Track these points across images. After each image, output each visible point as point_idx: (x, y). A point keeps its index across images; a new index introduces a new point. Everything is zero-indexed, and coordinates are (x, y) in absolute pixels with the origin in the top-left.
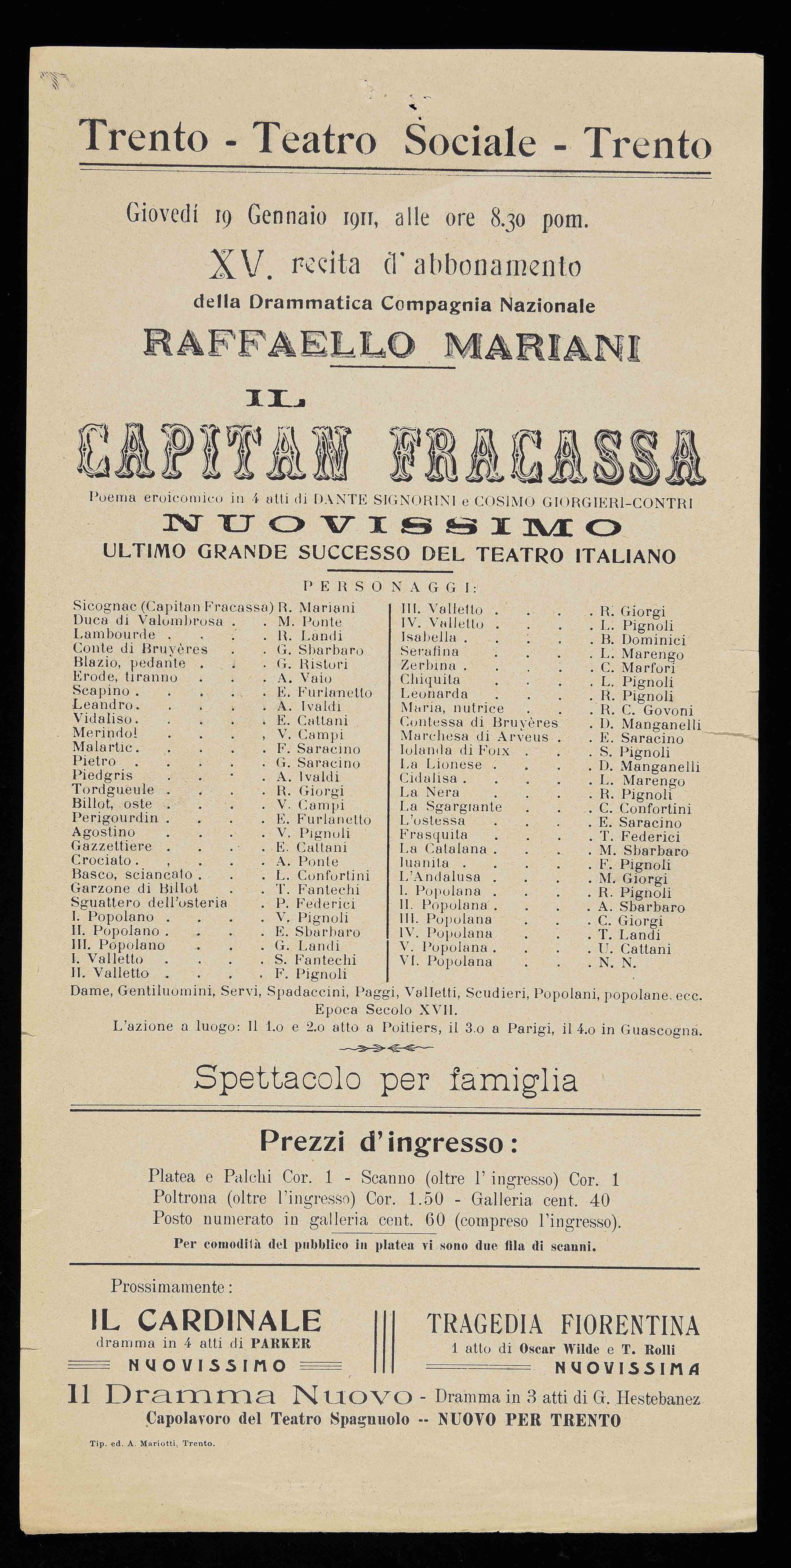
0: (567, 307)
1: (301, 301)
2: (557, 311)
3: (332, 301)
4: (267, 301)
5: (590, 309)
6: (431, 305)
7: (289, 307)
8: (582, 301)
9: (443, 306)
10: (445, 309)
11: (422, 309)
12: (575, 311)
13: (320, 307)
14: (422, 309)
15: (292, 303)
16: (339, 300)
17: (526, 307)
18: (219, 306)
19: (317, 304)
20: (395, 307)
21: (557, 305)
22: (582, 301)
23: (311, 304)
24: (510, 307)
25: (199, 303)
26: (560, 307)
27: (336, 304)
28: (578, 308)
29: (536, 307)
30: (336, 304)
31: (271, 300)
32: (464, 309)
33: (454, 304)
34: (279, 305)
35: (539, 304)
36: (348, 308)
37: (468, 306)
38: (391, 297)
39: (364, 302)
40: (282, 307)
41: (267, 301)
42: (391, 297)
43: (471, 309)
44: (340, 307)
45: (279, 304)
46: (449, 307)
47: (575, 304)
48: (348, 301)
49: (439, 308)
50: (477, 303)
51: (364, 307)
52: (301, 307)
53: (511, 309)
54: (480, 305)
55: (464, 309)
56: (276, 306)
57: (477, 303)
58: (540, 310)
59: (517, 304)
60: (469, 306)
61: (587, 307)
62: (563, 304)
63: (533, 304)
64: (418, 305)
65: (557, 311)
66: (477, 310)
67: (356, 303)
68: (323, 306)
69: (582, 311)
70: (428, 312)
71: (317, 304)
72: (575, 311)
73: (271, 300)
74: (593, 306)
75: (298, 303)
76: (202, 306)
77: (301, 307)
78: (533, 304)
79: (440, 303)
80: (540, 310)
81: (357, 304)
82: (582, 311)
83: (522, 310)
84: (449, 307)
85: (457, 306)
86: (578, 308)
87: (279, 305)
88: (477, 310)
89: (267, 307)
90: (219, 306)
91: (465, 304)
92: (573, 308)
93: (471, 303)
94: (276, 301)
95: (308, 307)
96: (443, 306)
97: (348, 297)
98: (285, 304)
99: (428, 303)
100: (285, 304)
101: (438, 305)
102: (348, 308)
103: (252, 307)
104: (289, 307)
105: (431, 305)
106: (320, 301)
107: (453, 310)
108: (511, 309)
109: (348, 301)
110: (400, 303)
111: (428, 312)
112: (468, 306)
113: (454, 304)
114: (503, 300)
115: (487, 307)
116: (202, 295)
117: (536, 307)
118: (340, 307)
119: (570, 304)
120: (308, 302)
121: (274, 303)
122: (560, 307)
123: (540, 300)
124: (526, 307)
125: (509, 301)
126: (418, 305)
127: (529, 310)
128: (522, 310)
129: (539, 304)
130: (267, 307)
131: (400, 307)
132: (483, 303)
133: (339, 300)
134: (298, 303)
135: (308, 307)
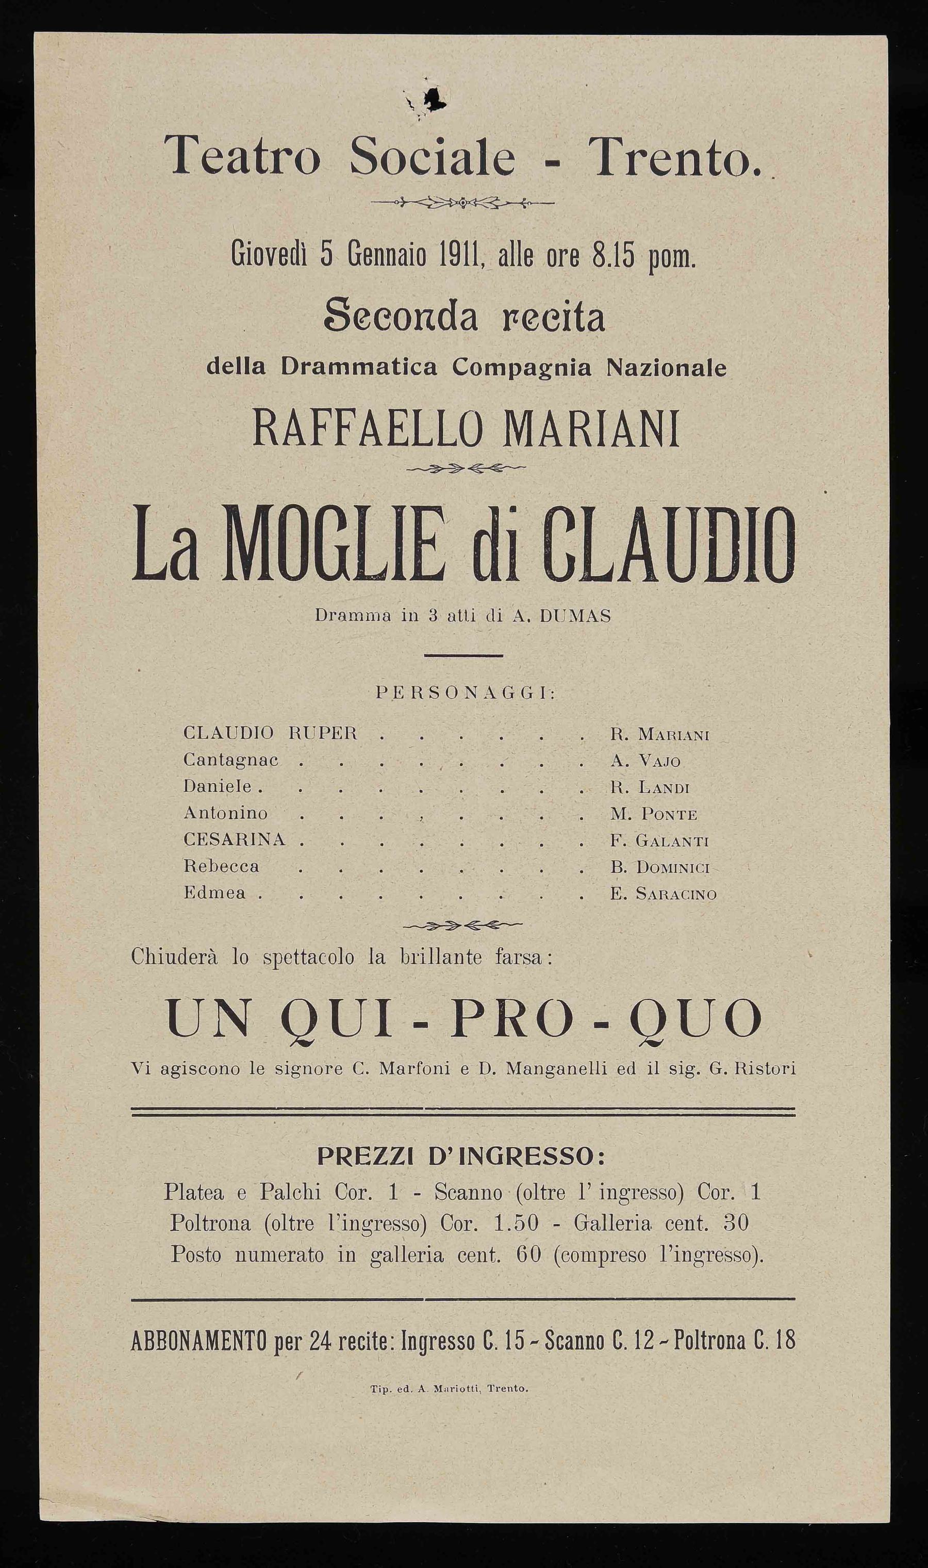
0: (691, 369)
1: (346, 365)
2: (679, 374)
3: (386, 364)
4: (304, 365)
5: (721, 372)
6: (515, 369)
7: (331, 372)
8: (710, 361)
9: (531, 369)
10: (534, 373)
11: (503, 373)
12: (702, 374)
13: (371, 373)
14: (503, 373)
15: (335, 368)
16: (395, 363)
17: (640, 370)
18: (239, 372)
19: (367, 368)
20: (469, 371)
21: (678, 366)
22: (710, 361)
23: (359, 368)
24: (619, 370)
25: (213, 368)
26: (683, 369)
27: (390, 368)
28: (706, 371)
29: (652, 370)
30: (390, 368)
31: (309, 364)
32: (557, 373)
33: (544, 368)
34: (318, 370)
35: (656, 366)
36: (406, 373)
37: (561, 369)
38: (466, 359)
39: (427, 365)
40: (323, 372)
41: (304, 365)
42: (466, 359)
43: (565, 374)
44: (396, 373)
45: (319, 369)
46: (538, 372)
47: (701, 366)
48: (406, 365)
49: (526, 373)
50: (573, 366)
51: (426, 371)
52: (347, 373)
53: (620, 373)
54: (577, 369)
55: (557, 373)
56: (314, 371)
57: (573, 366)
58: (657, 374)
59: (628, 366)
60: (563, 369)
61: (717, 369)
62: (686, 366)
63: (648, 365)
64: (499, 369)
65: (679, 374)
66: (573, 374)
67: (416, 367)
68: (375, 371)
69: (710, 374)
70: (511, 378)
71: (367, 368)
72: (702, 374)
73: (309, 364)
74: (724, 368)
75: (343, 368)
76: (217, 372)
77: (347, 373)
78: (648, 365)
79: (527, 365)
80: (657, 374)
81: (417, 368)
82: (710, 374)
83: (635, 374)
84: (538, 372)
85: (548, 369)
86: (706, 371)
87: (318, 370)
88: (573, 374)
89: (304, 372)
90: (239, 372)
91: (557, 366)
92: (698, 371)
93: (565, 365)
94: (316, 364)
95: (355, 373)
96: (531, 369)
97: (406, 359)
98: (326, 370)
99: (511, 365)
100: (326, 370)
101: (523, 368)
102: (406, 373)
103: (284, 372)
104: (331, 372)
105: (515, 369)
106: (371, 364)
107: (543, 374)
108: (620, 373)
109: (406, 365)
110: (476, 366)
111: (511, 378)
112: (561, 369)
113: (544, 368)
114: (611, 361)
115: (586, 370)
116: (217, 358)
117: (652, 370)
118: (396, 373)
119: (695, 366)
120: (355, 365)
121: (313, 367)
122: (683, 369)
123: (657, 360)
124: (640, 370)
125: (617, 363)
126: (499, 369)
127: (643, 374)
128: (635, 374)
129: (656, 366)
130: (304, 372)
131: (476, 370)
132: (581, 365)
133: (395, 363)
134: (343, 368)
135: (355, 373)
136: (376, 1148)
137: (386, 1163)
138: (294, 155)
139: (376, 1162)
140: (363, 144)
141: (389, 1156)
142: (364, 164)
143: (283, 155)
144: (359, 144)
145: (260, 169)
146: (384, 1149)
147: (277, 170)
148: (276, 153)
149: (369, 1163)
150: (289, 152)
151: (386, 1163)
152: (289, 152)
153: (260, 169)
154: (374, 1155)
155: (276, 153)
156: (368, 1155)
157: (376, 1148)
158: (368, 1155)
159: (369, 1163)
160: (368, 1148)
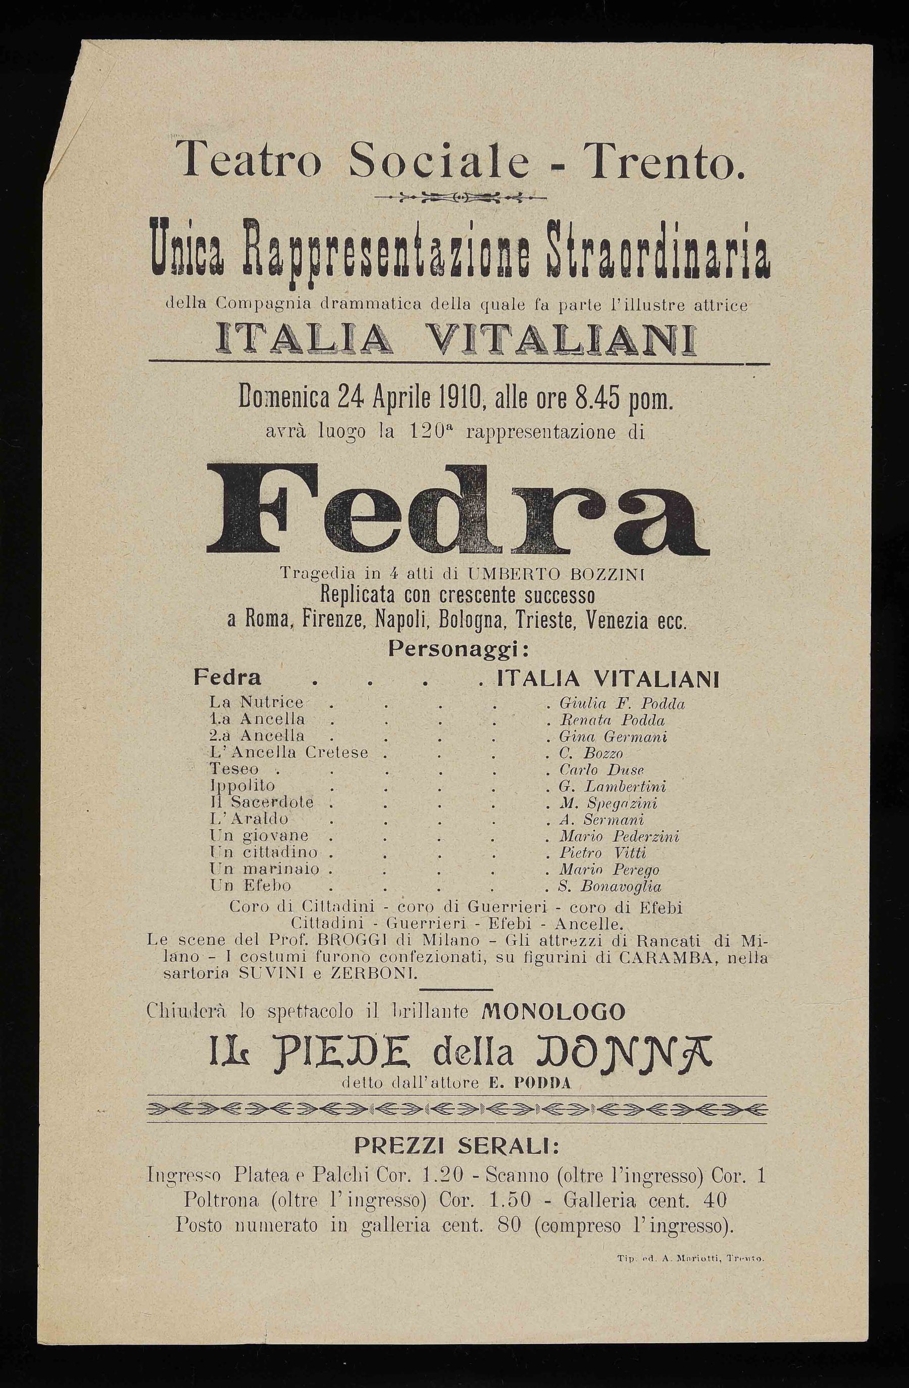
136: (409, 1139)
137: (418, 1152)
138: (297, 159)
139: (409, 1152)
140: (362, 150)
141: (421, 1145)
142: (363, 168)
143: (286, 159)
144: (359, 149)
145: (265, 173)
146: (417, 1139)
147: (281, 173)
148: (280, 157)
149: (402, 1152)
150: (292, 156)
151: (418, 1152)
152: (292, 156)
153: (265, 173)
154: (407, 1145)
155: (280, 157)
156: (401, 1145)
157: (409, 1139)
158: (401, 1145)
159: (402, 1152)
160: (402, 1138)
